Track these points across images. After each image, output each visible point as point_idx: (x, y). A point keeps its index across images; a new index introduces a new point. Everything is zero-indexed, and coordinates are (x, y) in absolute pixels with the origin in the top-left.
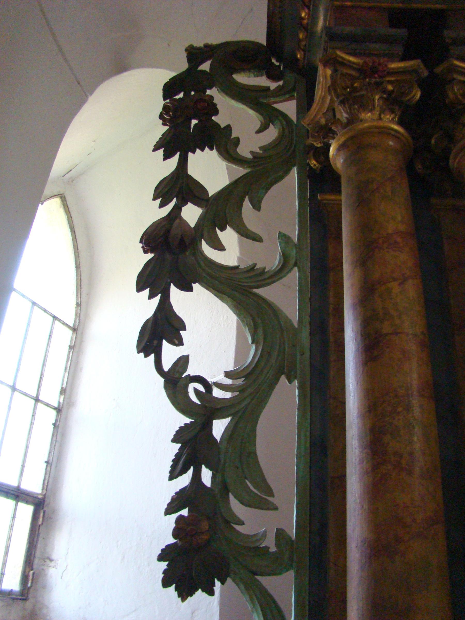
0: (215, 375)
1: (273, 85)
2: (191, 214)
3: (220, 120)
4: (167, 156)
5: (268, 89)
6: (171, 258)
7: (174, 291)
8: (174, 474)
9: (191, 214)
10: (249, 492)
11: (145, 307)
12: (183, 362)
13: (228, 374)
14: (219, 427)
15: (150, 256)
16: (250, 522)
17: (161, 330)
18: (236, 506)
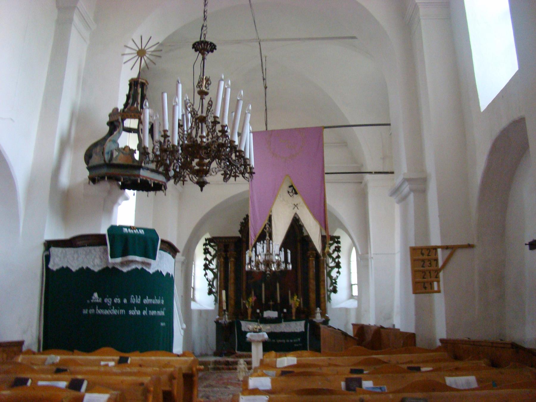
6: (206, 267)
11: (204, 272)
16: (214, 290)
17: (206, 274)
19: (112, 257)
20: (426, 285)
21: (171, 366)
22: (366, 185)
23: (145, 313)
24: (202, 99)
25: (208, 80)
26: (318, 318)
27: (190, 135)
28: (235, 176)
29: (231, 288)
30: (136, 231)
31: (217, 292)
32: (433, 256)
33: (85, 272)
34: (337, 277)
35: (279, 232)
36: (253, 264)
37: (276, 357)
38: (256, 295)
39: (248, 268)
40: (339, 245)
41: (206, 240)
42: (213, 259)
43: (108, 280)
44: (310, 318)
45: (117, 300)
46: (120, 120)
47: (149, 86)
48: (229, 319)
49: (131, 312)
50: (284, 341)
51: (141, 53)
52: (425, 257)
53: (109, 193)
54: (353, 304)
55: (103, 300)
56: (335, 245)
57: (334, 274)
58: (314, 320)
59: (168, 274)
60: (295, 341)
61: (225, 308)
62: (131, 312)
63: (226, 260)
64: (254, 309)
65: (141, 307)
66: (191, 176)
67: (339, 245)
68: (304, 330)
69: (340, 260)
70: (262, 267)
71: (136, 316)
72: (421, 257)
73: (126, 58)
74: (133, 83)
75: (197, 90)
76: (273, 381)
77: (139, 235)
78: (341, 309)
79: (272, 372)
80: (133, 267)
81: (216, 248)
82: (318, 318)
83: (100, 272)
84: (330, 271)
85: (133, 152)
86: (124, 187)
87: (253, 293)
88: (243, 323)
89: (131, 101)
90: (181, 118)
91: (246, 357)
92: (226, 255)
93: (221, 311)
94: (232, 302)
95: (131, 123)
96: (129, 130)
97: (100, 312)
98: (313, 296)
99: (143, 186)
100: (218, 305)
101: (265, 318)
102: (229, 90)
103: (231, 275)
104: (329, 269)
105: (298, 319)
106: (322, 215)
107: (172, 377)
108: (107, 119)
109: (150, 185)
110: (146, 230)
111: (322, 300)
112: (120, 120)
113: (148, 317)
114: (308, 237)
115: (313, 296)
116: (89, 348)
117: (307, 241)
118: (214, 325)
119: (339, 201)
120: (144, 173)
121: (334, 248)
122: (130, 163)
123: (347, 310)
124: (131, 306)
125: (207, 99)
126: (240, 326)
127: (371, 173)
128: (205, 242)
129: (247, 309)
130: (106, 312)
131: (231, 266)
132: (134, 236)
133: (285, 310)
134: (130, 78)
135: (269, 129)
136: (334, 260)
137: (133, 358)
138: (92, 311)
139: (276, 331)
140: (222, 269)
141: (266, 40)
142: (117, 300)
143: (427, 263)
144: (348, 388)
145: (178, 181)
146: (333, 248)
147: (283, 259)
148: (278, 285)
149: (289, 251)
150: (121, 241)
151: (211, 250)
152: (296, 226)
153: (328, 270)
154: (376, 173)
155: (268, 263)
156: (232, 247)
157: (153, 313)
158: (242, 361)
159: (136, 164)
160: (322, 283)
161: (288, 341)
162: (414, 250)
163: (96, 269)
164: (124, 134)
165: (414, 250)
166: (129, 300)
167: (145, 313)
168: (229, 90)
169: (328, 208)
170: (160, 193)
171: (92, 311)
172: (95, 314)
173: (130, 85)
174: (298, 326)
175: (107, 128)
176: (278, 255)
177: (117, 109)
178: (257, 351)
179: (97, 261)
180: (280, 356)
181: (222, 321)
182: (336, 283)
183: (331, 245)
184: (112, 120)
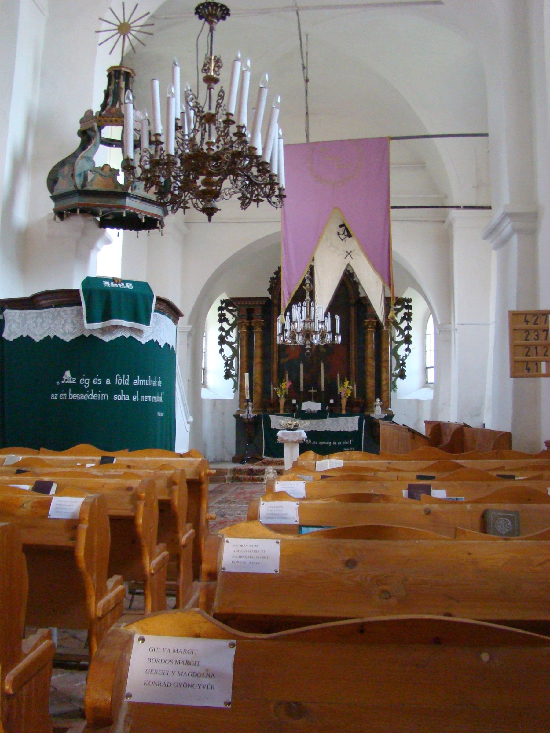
0: (228, 356)
1: (234, 309)
2: (224, 334)
6: (222, 340)
11: (219, 347)
14: (229, 362)
16: (233, 372)
17: (222, 350)
19: (89, 321)
20: (531, 366)
21: (171, 468)
22: (451, 226)
23: (135, 398)
24: (210, 89)
25: (217, 61)
26: (378, 413)
27: (192, 140)
28: (258, 201)
29: (257, 369)
30: (121, 285)
31: (237, 375)
32: (542, 325)
33: (52, 343)
34: (406, 356)
35: (325, 290)
36: (287, 334)
37: (315, 459)
38: (290, 379)
39: (279, 340)
40: (410, 311)
41: (222, 302)
42: (231, 329)
43: (83, 353)
44: (366, 413)
45: (97, 381)
46: (96, 128)
47: (136, 78)
48: (253, 412)
49: (116, 397)
50: (329, 443)
51: (124, 29)
52: (530, 326)
53: (84, 233)
54: (427, 395)
55: (78, 381)
56: (405, 311)
57: (401, 351)
58: (372, 415)
59: (167, 346)
61: (248, 397)
62: (116, 397)
63: (250, 329)
64: (288, 398)
65: (130, 390)
66: (194, 200)
67: (410, 311)
68: (357, 429)
69: (410, 332)
70: (300, 340)
71: (123, 402)
72: (524, 326)
73: (103, 36)
74: (113, 73)
75: (202, 75)
76: (307, 487)
77: (126, 292)
78: (410, 401)
79: (309, 477)
80: (119, 335)
81: (236, 313)
82: (378, 413)
83: (72, 341)
84: (396, 348)
85: (115, 172)
86: (104, 224)
87: (287, 376)
88: (273, 418)
89: (110, 100)
90: (179, 116)
91: (276, 463)
92: (250, 323)
94: (258, 389)
95: (111, 132)
96: (110, 143)
97: (74, 396)
98: (371, 382)
99: (131, 222)
100: (238, 392)
101: (304, 411)
102: (248, 75)
103: (257, 352)
104: (394, 345)
105: (350, 413)
106: (386, 268)
107: (171, 483)
108: (78, 127)
109: (141, 220)
110: (135, 283)
111: (384, 388)
112: (96, 128)
113: (140, 403)
114: (366, 298)
115: (371, 382)
116: (61, 445)
117: (364, 304)
118: (234, 419)
119: (410, 247)
120: (130, 203)
121: (403, 316)
122: (111, 189)
123: (418, 402)
124: (115, 389)
125: (216, 88)
126: (268, 422)
127: (458, 207)
128: (220, 305)
129: (278, 399)
130: (83, 397)
131: (257, 340)
132: (119, 291)
133: (332, 401)
134: (108, 67)
135: (311, 140)
136: (402, 332)
137: (121, 458)
138: (63, 396)
139: (318, 429)
140: (244, 343)
141: (307, 8)
142: (97, 381)
143: (533, 335)
144: (411, 496)
145: (177, 209)
146: (401, 315)
147: (329, 328)
148: (322, 366)
149: (338, 318)
150: (102, 299)
151: (229, 316)
152: (349, 283)
153: (393, 347)
154: (465, 207)
155: (307, 334)
156: (258, 313)
157: (147, 398)
158: (270, 468)
159: (119, 190)
160: (384, 364)
161: (335, 443)
162: (514, 315)
163: (68, 339)
164: (102, 147)
165: (514, 315)
166: (113, 381)
167: (135, 398)
168: (248, 75)
169: (394, 257)
170: (154, 232)
171: (63, 396)
172: (68, 401)
173: (109, 76)
174: (350, 424)
175: (79, 140)
176: (323, 322)
177: (91, 112)
178: (291, 454)
179: (69, 327)
180: (320, 459)
181: (244, 415)
182: (404, 364)
183: (399, 310)
184: (84, 128)
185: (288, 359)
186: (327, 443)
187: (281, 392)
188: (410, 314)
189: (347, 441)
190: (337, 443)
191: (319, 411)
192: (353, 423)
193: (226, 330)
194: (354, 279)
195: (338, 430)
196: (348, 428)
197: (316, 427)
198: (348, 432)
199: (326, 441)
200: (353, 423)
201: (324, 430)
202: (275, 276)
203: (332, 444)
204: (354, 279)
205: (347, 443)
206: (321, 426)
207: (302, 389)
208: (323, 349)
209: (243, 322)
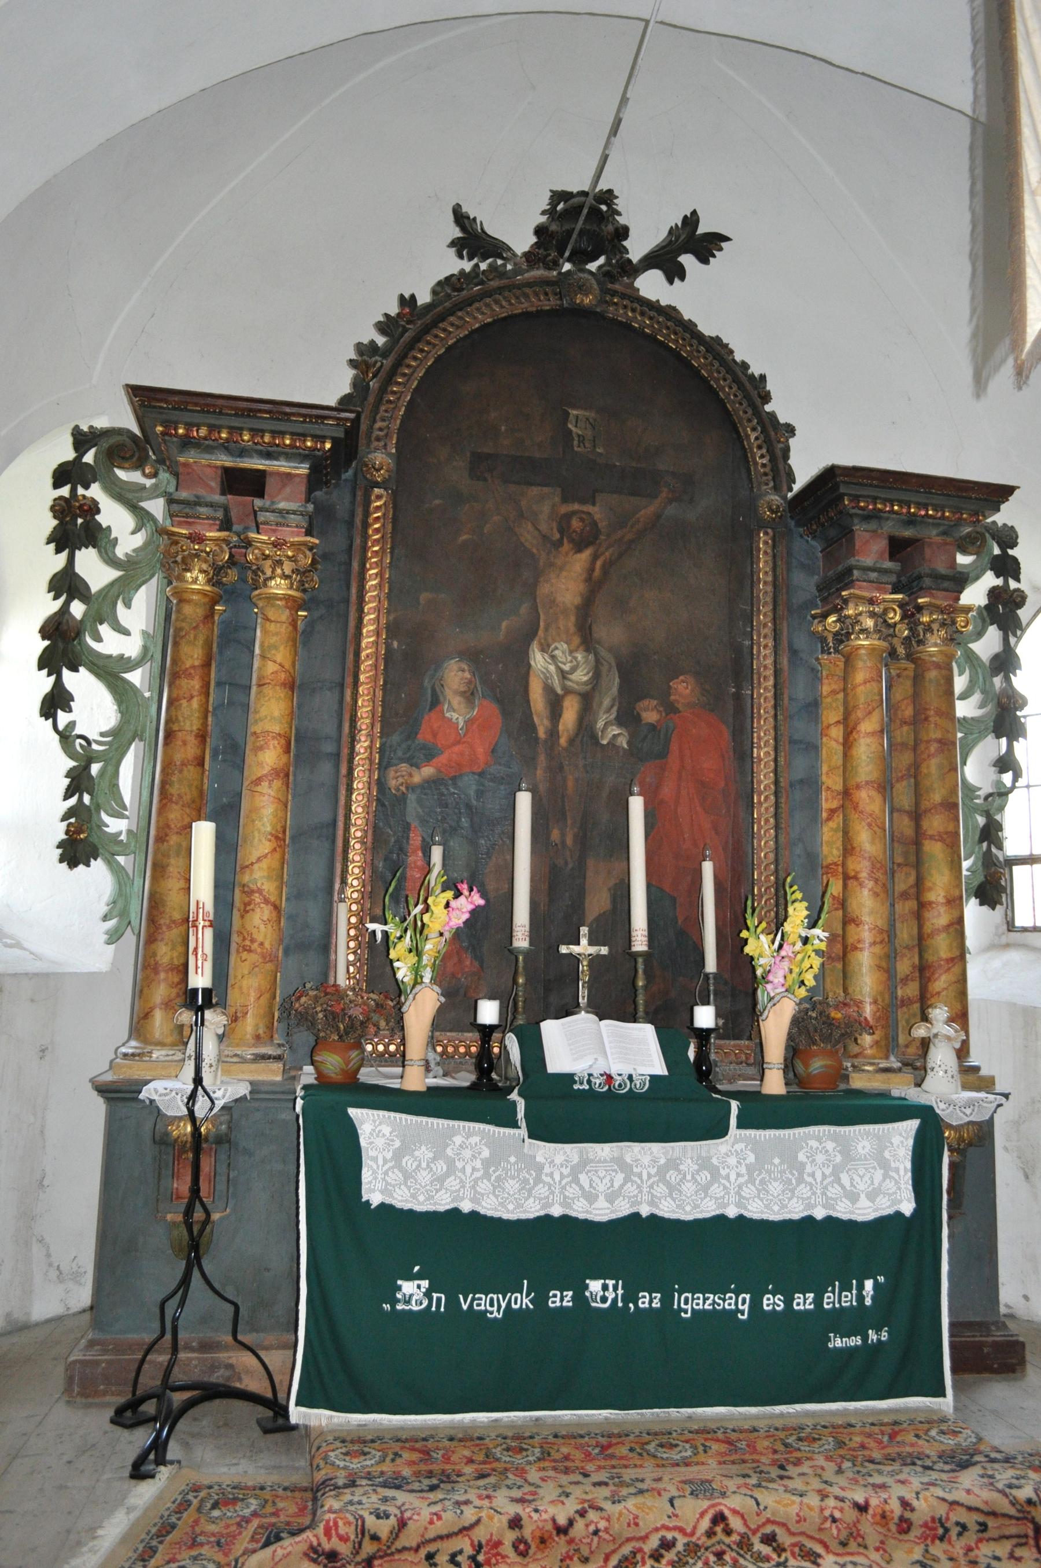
1: (149, 483)
3: (102, 519)
4: (58, 551)
5: (143, 488)
6: (63, 644)
7: (65, 672)
8: (66, 797)
9: (77, 609)
10: (113, 809)
11: (45, 683)
12: (72, 725)
13: (102, 734)
15: (47, 643)
16: (115, 825)
17: (56, 702)
18: (104, 817)
29: (264, 810)
34: (1002, 794)
40: (1013, 584)
41: (82, 440)
42: (122, 590)
56: (990, 579)
60: (829, 1301)
67: (1013, 584)
68: (908, 1207)
93: (168, 997)
94: (260, 924)
128: (70, 455)
131: (273, 650)
139: (668, 1210)
146: (975, 595)
148: (637, 805)
185: (428, 771)
186: (729, 1302)
187: (416, 950)
188: (1018, 600)
189: (846, 1287)
190: (789, 1301)
191: (654, 1078)
192: (884, 1165)
193: (94, 588)
194: (768, 408)
195: (795, 1211)
196: (853, 1197)
197: (661, 1189)
198: (852, 1224)
199: (721, 1290)
200: (884, 1165)
201: (708, 1210)
202: (381, 340)
203: (756, 1304)
204: (768, 408)
205: (848, 1299)
206: (689, 1188)
207: (521, 940)
208: (615, 730)
209: (200, 539)
